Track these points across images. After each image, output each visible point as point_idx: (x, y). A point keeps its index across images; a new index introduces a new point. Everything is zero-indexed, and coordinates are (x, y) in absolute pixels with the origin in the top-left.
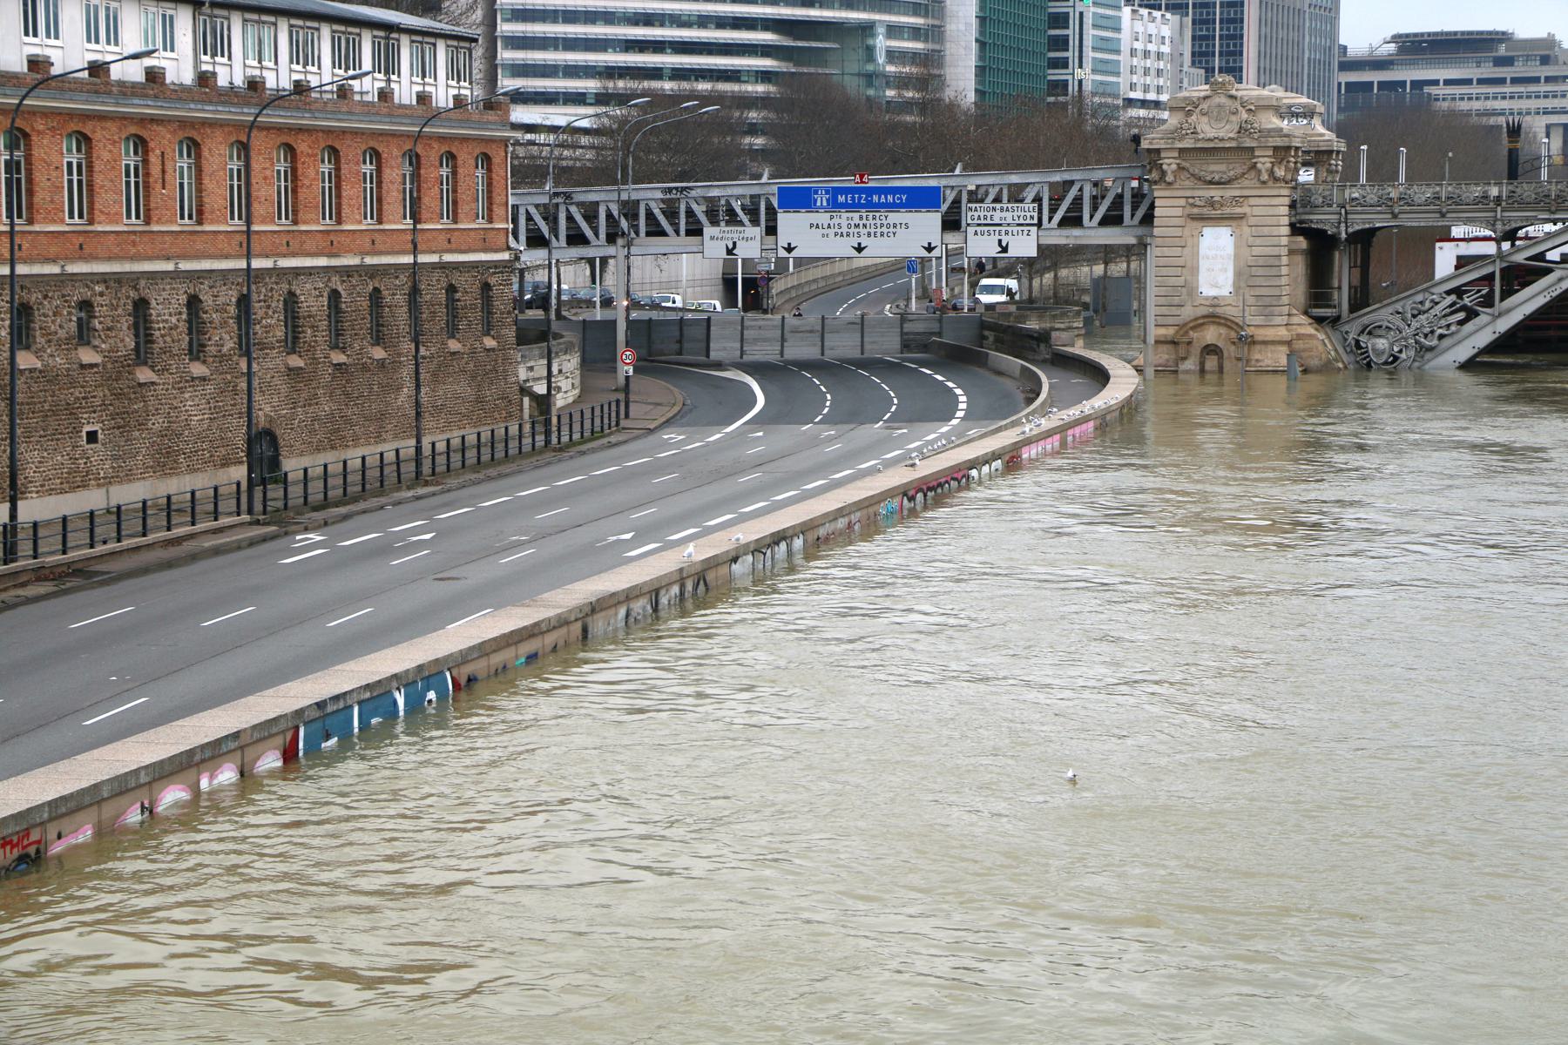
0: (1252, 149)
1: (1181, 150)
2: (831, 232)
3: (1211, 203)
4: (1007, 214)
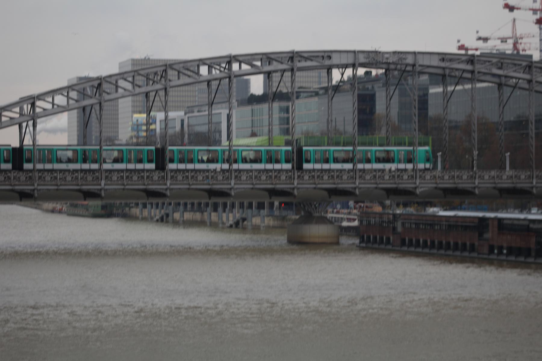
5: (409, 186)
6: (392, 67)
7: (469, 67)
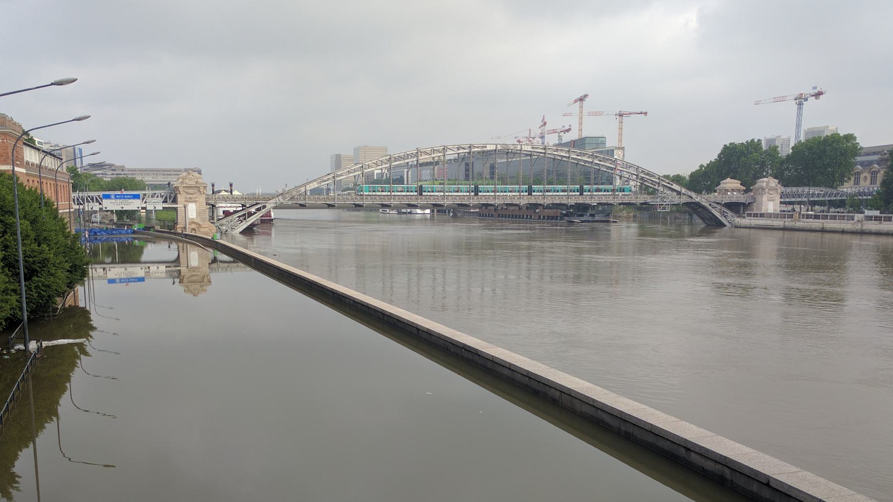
0: (199, 187)
1: (184, 187)
2: (115, 204)
3: (191, 198)
4: (155, 200)
5: (517, 202)
6: (510, 151)
7: (543, 151)
